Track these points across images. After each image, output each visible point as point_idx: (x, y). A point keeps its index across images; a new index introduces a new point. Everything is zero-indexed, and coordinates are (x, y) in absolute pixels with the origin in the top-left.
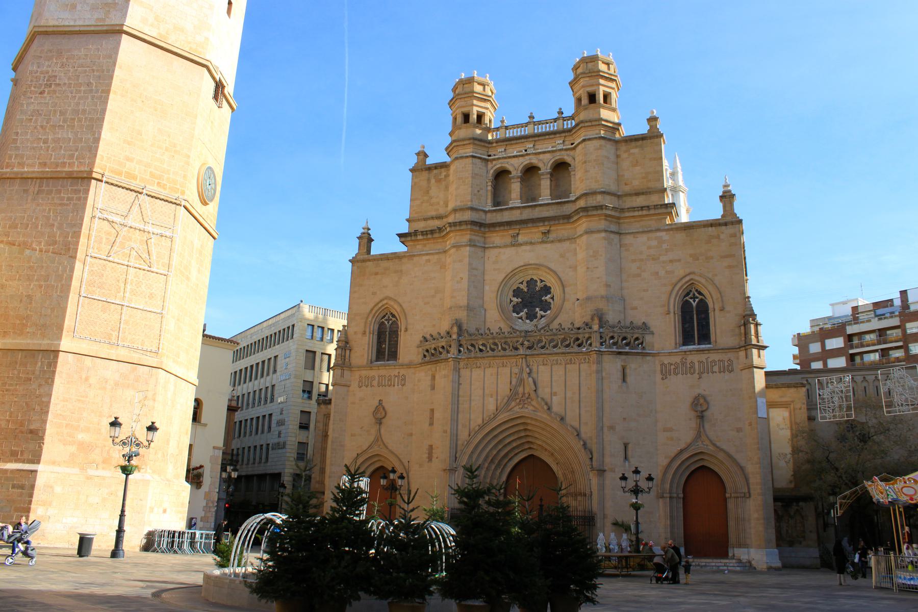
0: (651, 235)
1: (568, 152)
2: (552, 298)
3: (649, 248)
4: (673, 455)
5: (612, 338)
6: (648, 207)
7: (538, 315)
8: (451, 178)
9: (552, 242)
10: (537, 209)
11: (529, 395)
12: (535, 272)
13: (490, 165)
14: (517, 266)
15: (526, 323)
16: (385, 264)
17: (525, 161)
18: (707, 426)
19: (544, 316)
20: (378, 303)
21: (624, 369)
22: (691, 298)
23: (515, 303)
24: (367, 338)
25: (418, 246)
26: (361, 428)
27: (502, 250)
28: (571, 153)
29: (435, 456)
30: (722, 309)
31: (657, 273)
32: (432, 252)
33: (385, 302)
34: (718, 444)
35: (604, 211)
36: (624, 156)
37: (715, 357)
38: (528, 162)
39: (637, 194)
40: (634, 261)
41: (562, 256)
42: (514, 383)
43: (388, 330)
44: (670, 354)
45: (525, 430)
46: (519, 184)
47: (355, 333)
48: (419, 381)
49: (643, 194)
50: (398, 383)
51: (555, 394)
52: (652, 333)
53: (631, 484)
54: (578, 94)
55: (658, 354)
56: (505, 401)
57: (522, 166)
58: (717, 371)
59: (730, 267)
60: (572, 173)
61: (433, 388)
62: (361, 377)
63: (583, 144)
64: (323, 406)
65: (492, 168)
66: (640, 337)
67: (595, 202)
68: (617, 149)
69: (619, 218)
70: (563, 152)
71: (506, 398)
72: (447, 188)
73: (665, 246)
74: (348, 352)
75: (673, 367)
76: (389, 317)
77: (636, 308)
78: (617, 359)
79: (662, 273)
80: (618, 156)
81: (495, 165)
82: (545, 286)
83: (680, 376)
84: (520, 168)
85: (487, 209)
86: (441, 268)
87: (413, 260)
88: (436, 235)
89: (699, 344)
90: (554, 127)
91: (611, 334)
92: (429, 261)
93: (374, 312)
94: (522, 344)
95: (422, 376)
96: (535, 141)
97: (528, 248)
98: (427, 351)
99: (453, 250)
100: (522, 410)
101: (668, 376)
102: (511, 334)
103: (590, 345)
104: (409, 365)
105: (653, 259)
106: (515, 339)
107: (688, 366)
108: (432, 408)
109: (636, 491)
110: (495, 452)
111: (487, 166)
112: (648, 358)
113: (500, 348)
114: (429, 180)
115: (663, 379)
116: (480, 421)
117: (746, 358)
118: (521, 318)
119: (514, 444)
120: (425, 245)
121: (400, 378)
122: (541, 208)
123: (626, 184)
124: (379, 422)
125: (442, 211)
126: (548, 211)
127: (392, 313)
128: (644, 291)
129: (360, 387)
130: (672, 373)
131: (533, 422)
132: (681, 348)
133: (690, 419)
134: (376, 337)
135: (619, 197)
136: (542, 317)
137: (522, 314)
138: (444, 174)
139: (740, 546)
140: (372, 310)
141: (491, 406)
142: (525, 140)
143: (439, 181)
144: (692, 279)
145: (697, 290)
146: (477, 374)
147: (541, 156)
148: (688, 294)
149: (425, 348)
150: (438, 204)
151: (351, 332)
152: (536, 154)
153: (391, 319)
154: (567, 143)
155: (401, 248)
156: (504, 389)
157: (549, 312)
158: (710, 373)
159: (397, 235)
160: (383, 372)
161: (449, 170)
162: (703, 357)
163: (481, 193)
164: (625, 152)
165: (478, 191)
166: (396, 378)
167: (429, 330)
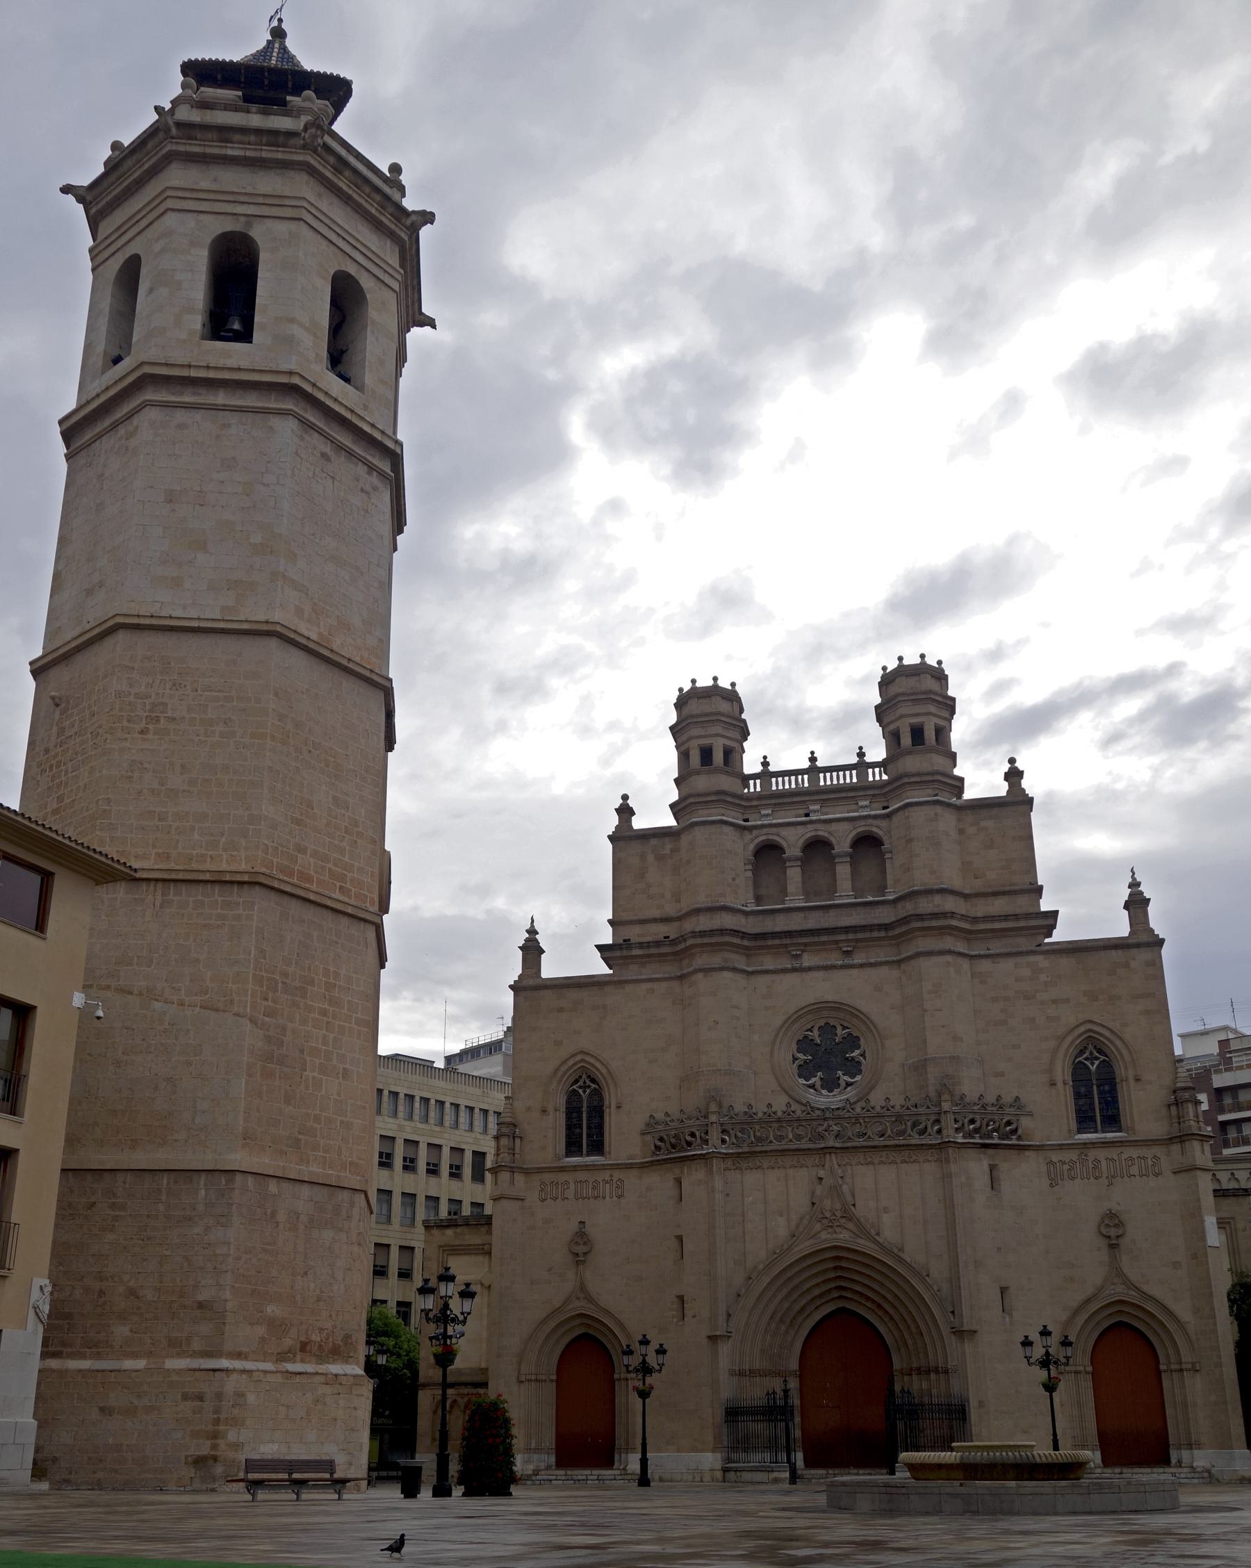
0: (1020, 959)
1: (878, 822)
2: (863, 1055)
3: (1017, 980)
5: (972, 1121)
7: (843, 1084)
9: (861, 966)
10: (832, 912)
15: (822, 1094)
16: (573, 994)
17: (808, 833)
19: (852, 1084)
20: (567, 1060)
21: (992, 1168)
22: (1086, 1059)
23: (802, 1063)
25: (631, 967)
26: (549, 1271)
28: (884, 823)
29: (689, 1313)
32: (657, 976)
33: (579, 1057)
34: (1145, 1288)
36: (971, 830)
38: (813, 834)
39: (996, 894)
42: (818, 1193)
43: (585, 1105)
44: (1061, 1147)
45: (835, 1268)
46: (799, 869)
47: (529, 1109)
49: (1004, 893)
50: (611, 1193)
51: (886, 1210)
52: (1030, 1114)
53: (1038, 1352)
54: (892, 727)
56: (805, 1222)
57: (802, 841)
58: (1136, 1173)
59: (1147, 1012)
60: (887, 856)
62: (542, 1183)
63: (907, 812)
64: (435, 1232)
65: (752, 840)
66: (1013, 1119)
67: (930, 905)
68: (959, 820)
70: (870, 821)
71: (807, 1217)
73: (1043, 977)
74: (518, 1141)
75: (1066, 1167)
76: (585, 1082)
77: (1002, 1074)
78: (982, 1156)
80: (961, 832)
81: (757, 837)
82: (850, 1034)
83: (1078, 1181)
85: (748, 909)
87: (624, 988)
89: (1103, 1132)
90: (852, 778)
91: (971, 1116)
92: (652, 991)
93: (560, 1074)
95: (659, 1183)
96: (823, 800)
97: (820, 974)
98: (661, 1139)
99: (700, 976)
100: (835, 1236)
101: (1060, 1182)
102: (809, 1114)
103: (939, 1131)
106: (815, 1123)
107: (1091, 1165)
108: (679, 1234)
109: (1045, 1363)
110: (786, 1305)
112: (1027, 1153)
113: (791, 1136)
114: (643, 857)
117: (1183, 1154)
119: (817, 1292)
121: (615, 1185)
123: (976, 877)
124: (579, 1259)
125: (671, 910)
127: (589, 1077)
129: (543, 1200)
130: (1066, 1177)
131: (851, 1256)
132: (1077, 1137)
133: (1099, 1249)
134: (564, 1114)
135: (966, 897)
136: (848, 1084)
138: (668, 847)
139: (1190, 1446)
140: (556, 1071)
142: (807, 798)
143: (660, 858)
144: (1090, 1030)
145: (1095, 1047)
146: (751, 1178)
147: (834, 826)
148: (1082, 1052)
149: (657, 1136)
152: (825, 821)
153: (589, 1087)
154: (874, 805)
157: (858, 1078)
158: (1126, 1178)
159: (597, 946)
160: (582, 1176)
162: (1113, 1153)
163: (737, 882)
165: (734, 879)
166: (608, 1186)
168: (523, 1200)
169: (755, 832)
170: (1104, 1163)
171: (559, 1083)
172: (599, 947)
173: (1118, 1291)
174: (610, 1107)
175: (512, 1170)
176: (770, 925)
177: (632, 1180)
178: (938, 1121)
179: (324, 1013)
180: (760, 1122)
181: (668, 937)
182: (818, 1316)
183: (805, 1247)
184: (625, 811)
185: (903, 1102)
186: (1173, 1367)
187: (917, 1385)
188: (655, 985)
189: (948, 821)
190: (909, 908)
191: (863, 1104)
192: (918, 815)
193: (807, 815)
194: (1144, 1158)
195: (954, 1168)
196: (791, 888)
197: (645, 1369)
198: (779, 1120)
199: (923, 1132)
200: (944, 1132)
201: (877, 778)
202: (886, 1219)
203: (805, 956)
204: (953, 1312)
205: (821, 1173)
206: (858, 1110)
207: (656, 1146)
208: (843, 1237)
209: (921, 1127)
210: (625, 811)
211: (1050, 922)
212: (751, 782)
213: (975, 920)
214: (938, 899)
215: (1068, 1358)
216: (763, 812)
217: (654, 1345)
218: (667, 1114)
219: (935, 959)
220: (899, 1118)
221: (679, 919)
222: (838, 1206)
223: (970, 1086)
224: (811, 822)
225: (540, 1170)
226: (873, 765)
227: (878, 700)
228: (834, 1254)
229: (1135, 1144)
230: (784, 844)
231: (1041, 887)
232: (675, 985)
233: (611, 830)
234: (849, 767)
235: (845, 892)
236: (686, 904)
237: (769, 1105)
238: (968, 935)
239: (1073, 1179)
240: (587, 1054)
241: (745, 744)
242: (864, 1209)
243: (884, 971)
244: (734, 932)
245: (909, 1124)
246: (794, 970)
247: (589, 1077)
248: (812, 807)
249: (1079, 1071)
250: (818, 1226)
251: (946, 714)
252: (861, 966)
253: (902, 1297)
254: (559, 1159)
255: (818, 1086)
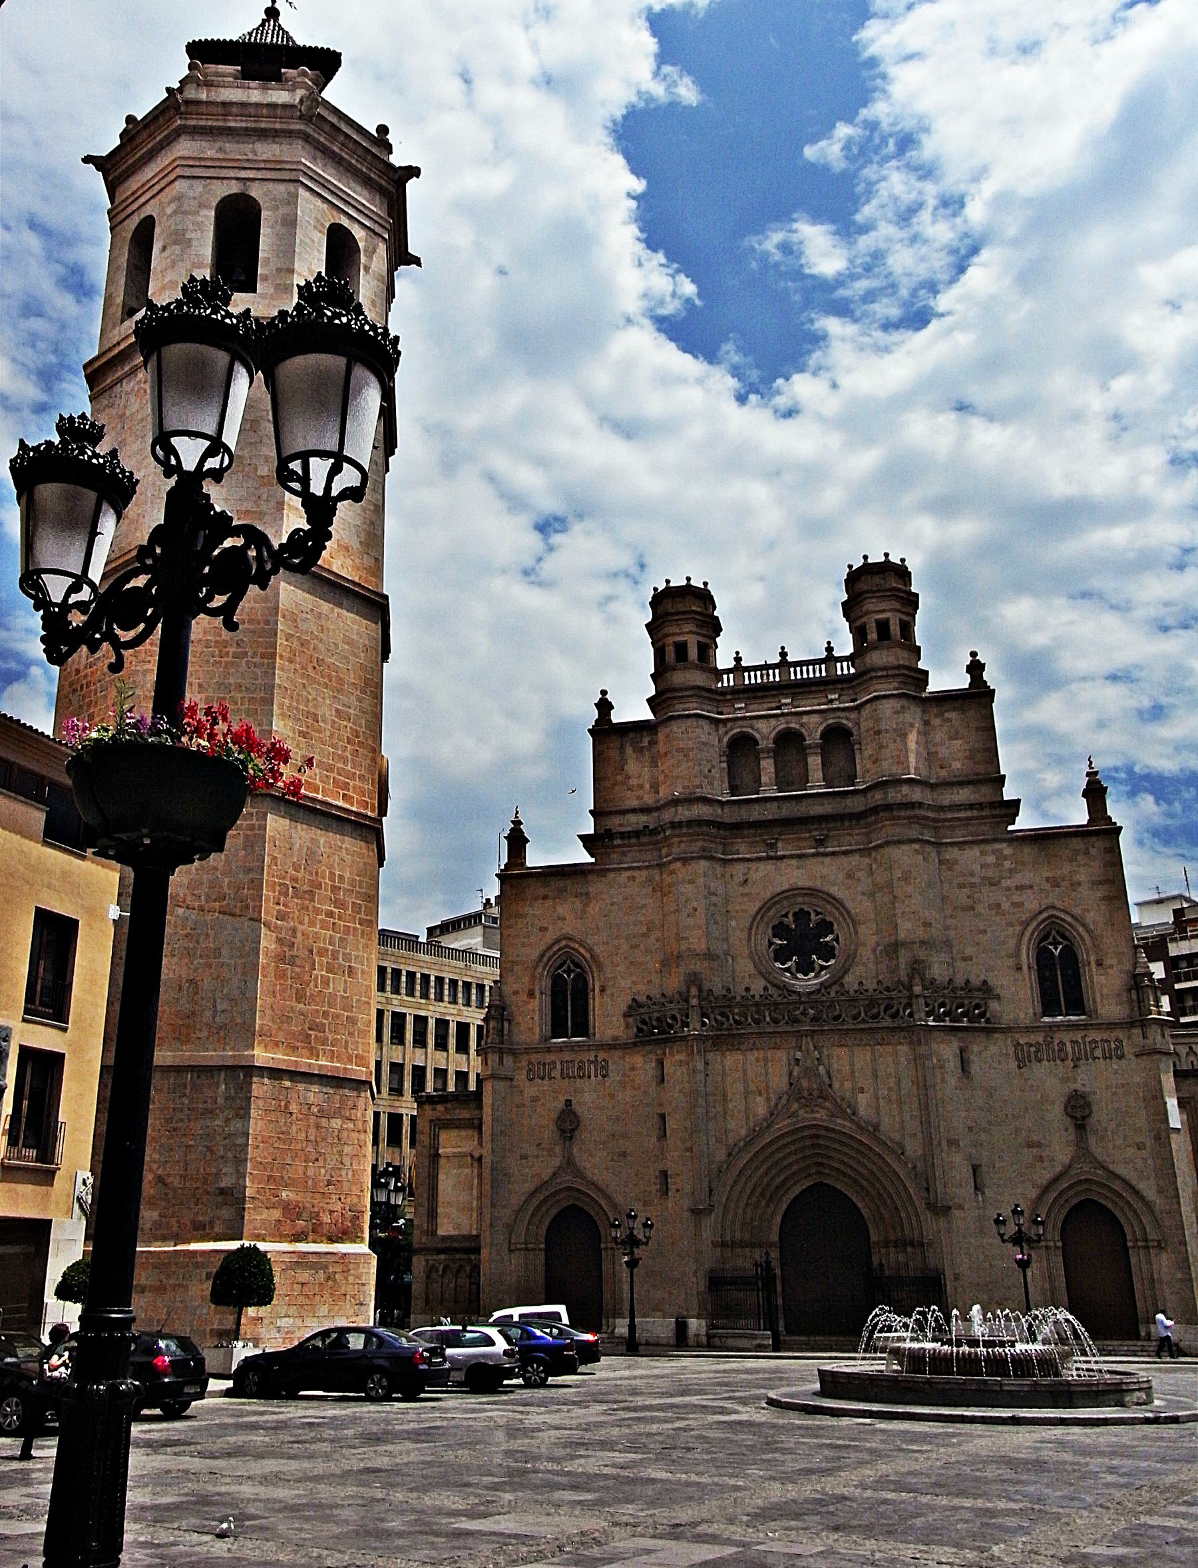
0: (983, 846)
2: (837, 939)
4: (1045, 1183)
5: (942, 1005)
6: (980, 804)
7: (817, 967)
8: (661, 747)
10: (805, 802)
11: (821, 1092)
12: (807, 899)
13: (722, 730)
14: (779, 890)
18: (1092, 1140)
20: (553, 944)
21: (962, 1051)
22: (1050, 944)
24: (537, 1002)
25: (613, 856)
27: (753, 865)
28: (853, 715)
29: (672, 1187)
30: (1099, 964)
31: (999, 905)
33: (564, 943)
34: (1111, 1167)
35: (918, 812)
37: (1094, 1035)
40: (960, 886)
41: (849, 876)
42: (795, 1073)
43: (570, 987)
44: (1028, 1030)
46: (771, 761)
47: (516, 993)
48: (633, 1069)
49: (969, 783)
51: (862, 1090)
52: (998, 997)
54: (858, 623)
55: (1007, 1030)
56: (784, 1101)
60: (856, 746)
61: (661, 1079)
62: (530, 1063)
68: (924, 711)
69: (935, 820)
70: (839, 714)
71: (785, 1097)
72: (654, 763)
73: (1007, 864)
74: (506, 1024)
75: (1033, 1049)
78: (953, 1038)
79: (1006, 906)
80: (926, 723)
81: (732, 729)
82: (823, 920)
83: (1045, 1063)
84: (772, 735)
86: (654, 890)
88: (645, 839)
91: (941, 1000)
92: (633, 878)
93: (545, 959)
94: (804, 1014)
95: (641, 1064)
97: (794, 862)
98: (644, 1022)
103: (911, 1015)
104: (613, 1046)
105: (991, 884)
110: (766, 1180)
111: (717, 730)
113: (768, 1019)
115: (1019, 1067)
116: (743, 1132)
118: (788, 970)
119: (795, 1168)
120: (624, 854)
122: (810, 801)
123: (941, 767)
125: (649, 800)
126: (823, 805)
127: (573, 962)
128: (980, 932)
129: (531, 1080)
133: (1067, 1130)
135: (933, 787)
136: (823, 968)
137: (789, 964)
140: (542, 956)
141: (762, 1110)
143: (640, 751)
145: (1058, 932)
146: (732, 1060)
147: (805, 719)
148: (1045, 938)
150: (641, 787)
151: (507, 989)
152: (796, 714)
154: (844, 698)
155: (585, 858)
156: (779, 1082)
157: (832, 962)
160: (567, 1056)
161: (656, 734)
164: (936, 716)
165: (710, 771)
167: (642, 991)
168: (511, 1079)
169: (729, 725)
170: (1068, 1044)
171: (544, 968)
172: (582, 837)
173: (1084, 1170)
174: (594, 990)
175: (501, 1052)
176: (745, 814)
177: (619, 1064)
178: (909, 1005)
179: (330, 914)
180: (740, 1005)
181: (647, 827)
182: (797, 1190)
183: (783, 1125)
184: (604, 706)
185: (875, 986)
186: (1140, 1244)
187: (894, 1257)
188: (636, 873)
189: (914, 715)
190: (878, 797)
191: (835, 988)
192: (887, 707)
193: (779, 708)
194: (1107, 1041)
195: (923, 1049)
196: (764, 779)
197: (632, 1242)
198: (757, 1004)
199: (894, 1016)
200: (916, 1017)
201: (846, 672)
202: (862, 1100)
203: (780, 845)
204: (927, 1189)
205: (799, 1055)
206: (833, 994)
207: (638, 1028)
208: (821, 1115)
209: (893, 1010)
210: (604, 706)
211: (1013, 811)
212: (725, 677)
213: (942, 809)
214: (905, 789)
215: (1039, 1236)
216: (737, 706)
217: (641, 1219)
218: (649, 997)
219: (905, 847)
220: (872, 1003)
221: (657, 809)
222: (815, 1086)
223: (938, 971)
224: (783, 715)
225: (528, 1051)
226: (841, 659)
227: (846, 597)
228: (814, 1131)
229: (1099, 1027)
230: (757, 736)
231: (1004, 776)
232: (657, 872)
233: (591, 724)
234: (820, 662)
235: (816, 784)
236: (664, 793)
237: (748, 989)
238: (935, 825)
239: (1040, 1061)
240: (571, 939)
241: (718, 639)
242: (843, 1087)
243: (855, 859)
244: (709, 823)
245: (882, 1007)
246: (769, 858)
247: (573, 962)
248: (784, 701)
249: (1043, 956)
250: (796, 1106)
251: (909, 610)
252: (833, 854)
253: (878, 1174)
254: (546, 1040)
255: (793, 970)
